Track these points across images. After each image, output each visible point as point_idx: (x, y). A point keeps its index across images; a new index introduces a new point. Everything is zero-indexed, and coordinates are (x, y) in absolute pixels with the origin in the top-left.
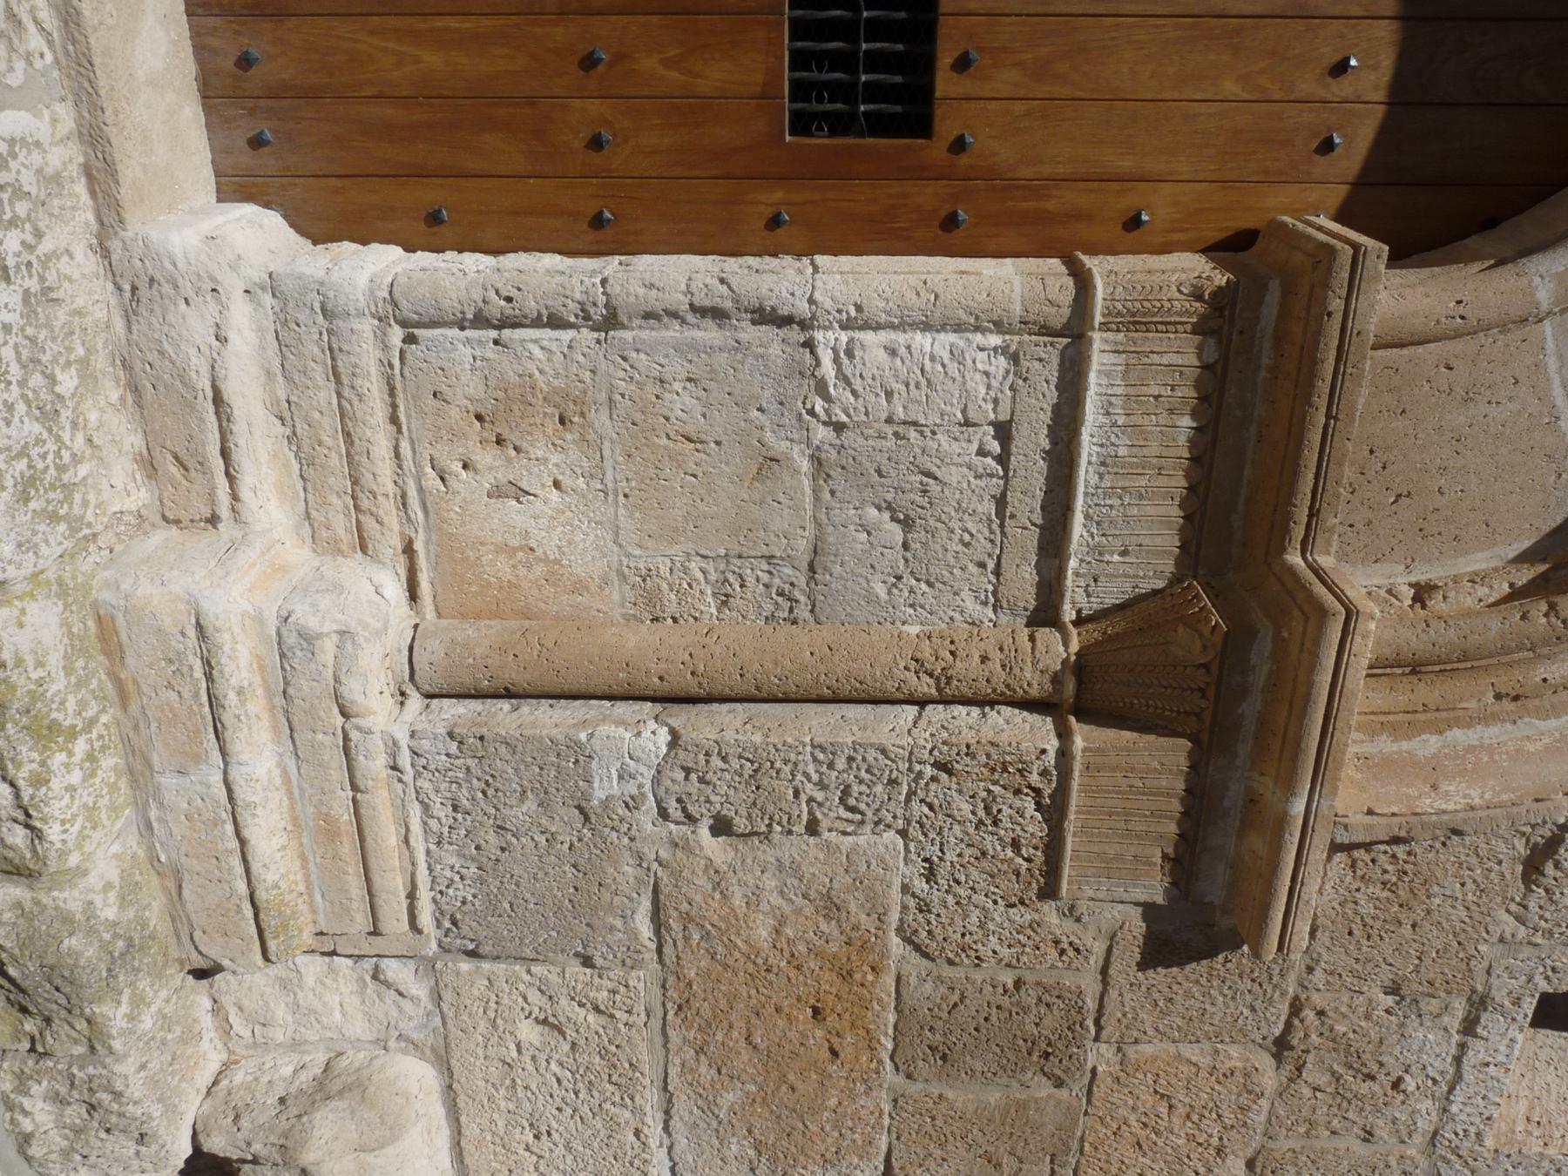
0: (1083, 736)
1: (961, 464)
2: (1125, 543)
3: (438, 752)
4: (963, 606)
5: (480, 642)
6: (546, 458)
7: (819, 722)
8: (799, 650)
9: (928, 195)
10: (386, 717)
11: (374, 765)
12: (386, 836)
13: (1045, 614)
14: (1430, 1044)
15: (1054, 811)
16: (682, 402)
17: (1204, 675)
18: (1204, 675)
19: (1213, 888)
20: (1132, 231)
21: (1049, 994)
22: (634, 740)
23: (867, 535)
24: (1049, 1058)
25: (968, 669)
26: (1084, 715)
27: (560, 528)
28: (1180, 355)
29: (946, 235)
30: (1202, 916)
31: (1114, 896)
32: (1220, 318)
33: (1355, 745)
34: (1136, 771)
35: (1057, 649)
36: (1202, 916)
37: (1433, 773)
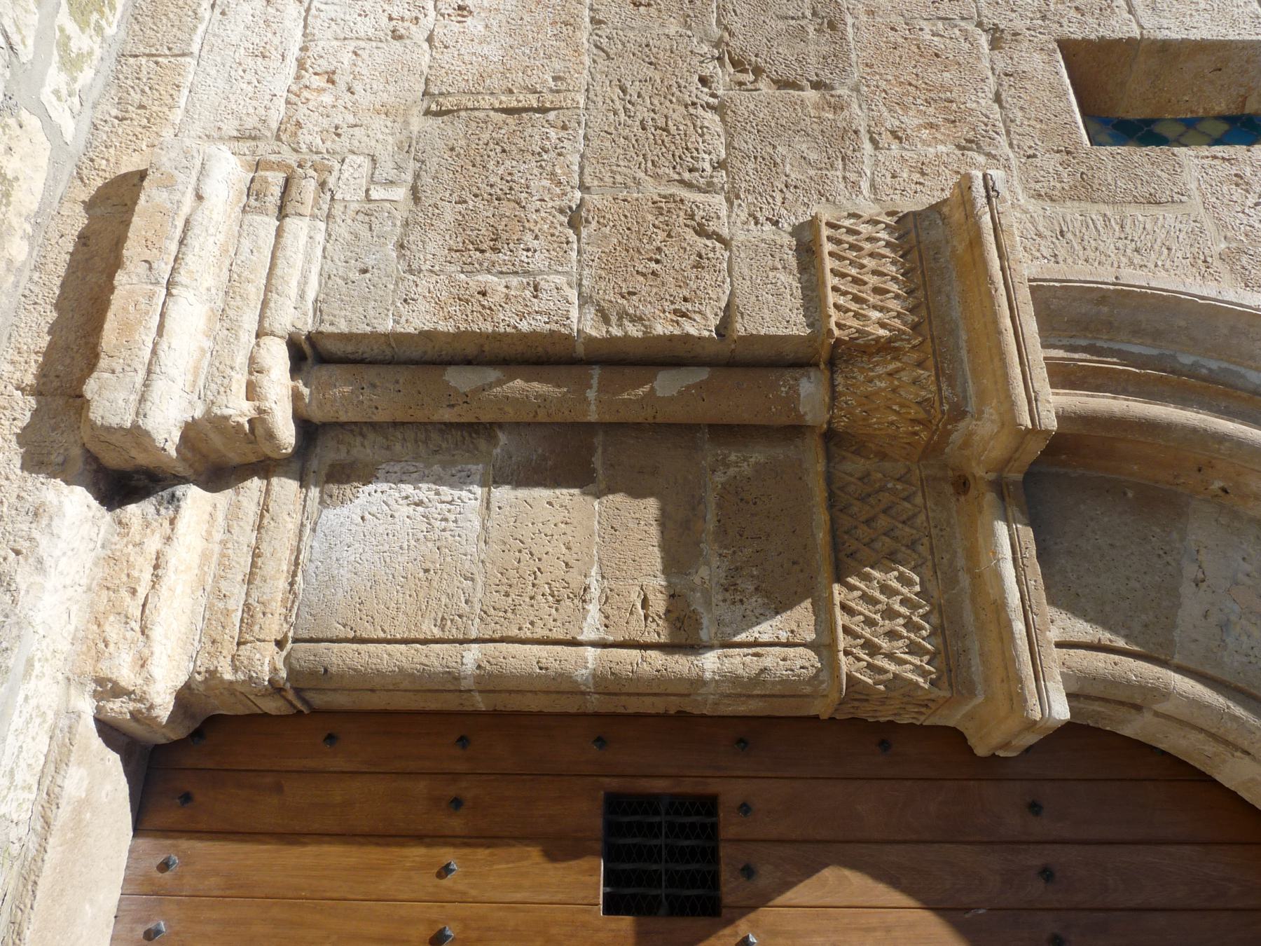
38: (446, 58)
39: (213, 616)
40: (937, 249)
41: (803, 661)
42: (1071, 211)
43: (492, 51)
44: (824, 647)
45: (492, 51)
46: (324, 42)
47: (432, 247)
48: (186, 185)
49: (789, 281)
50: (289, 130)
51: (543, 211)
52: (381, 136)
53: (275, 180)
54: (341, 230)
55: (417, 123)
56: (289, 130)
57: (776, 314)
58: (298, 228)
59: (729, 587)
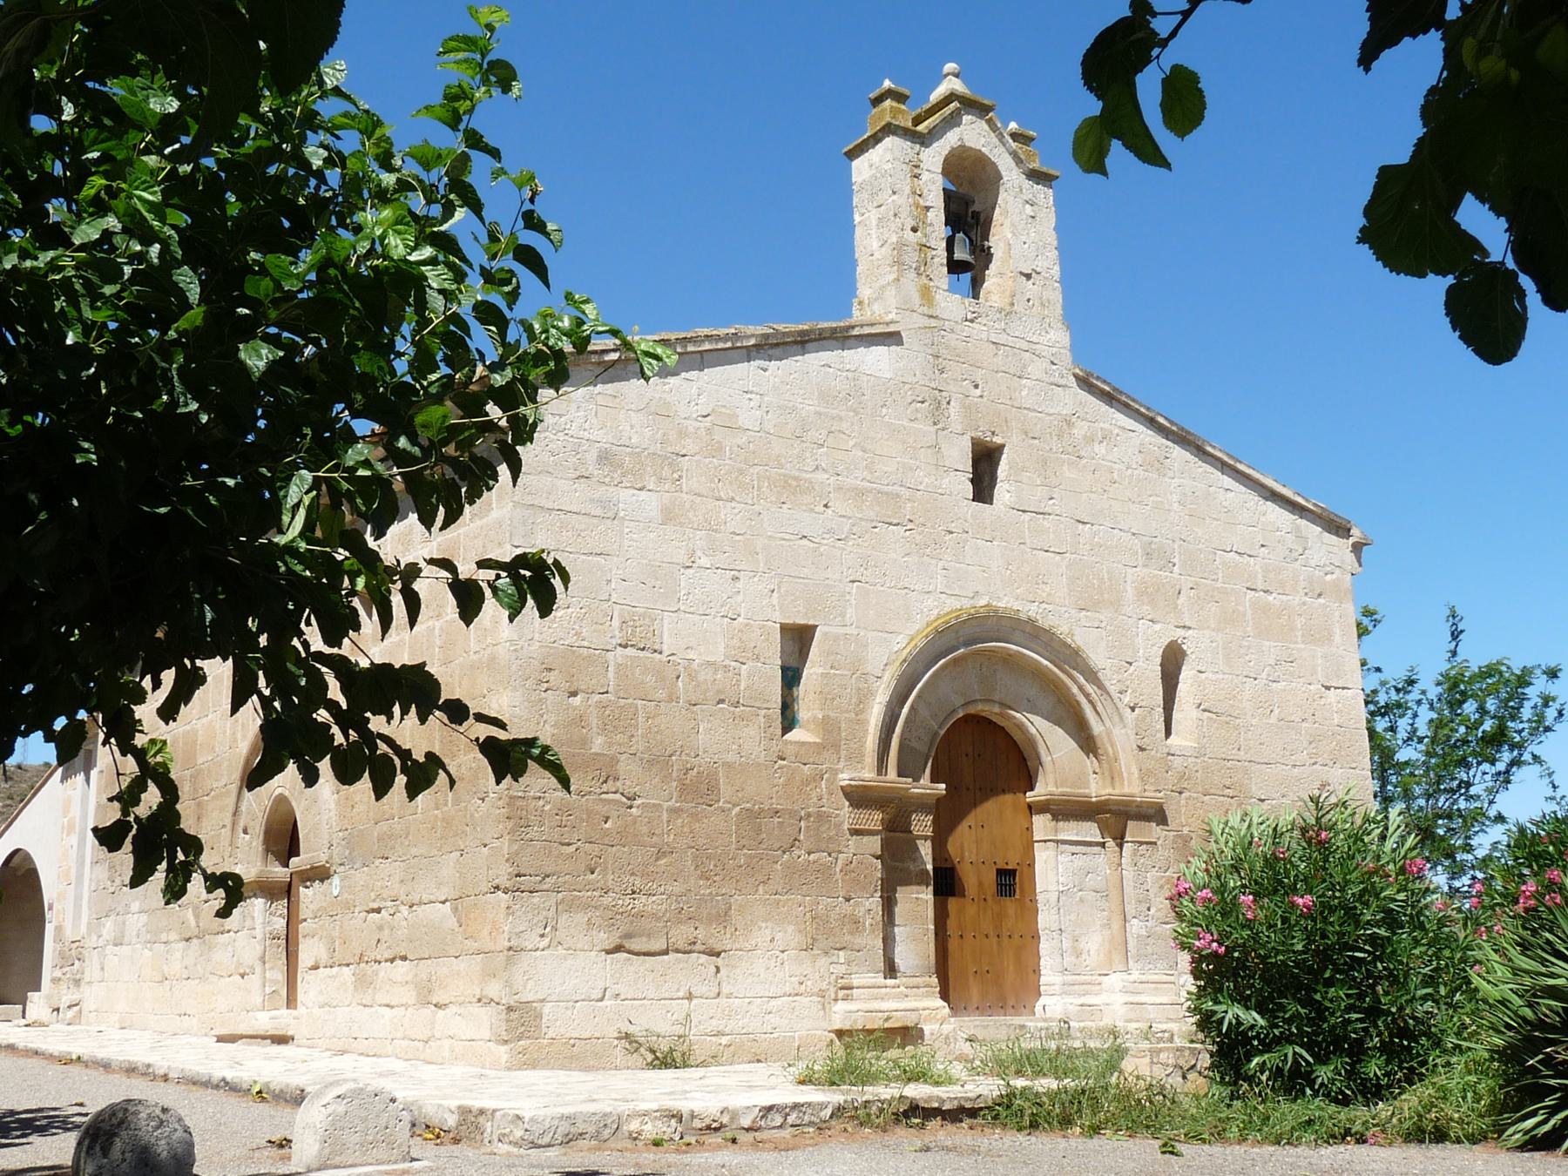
0: (1127, 838)
1: (1080, 861)
2: (1090, 831)
3: (1139, 965)
4: (1102, 861)
5: (1117, 957)
6: (1082, 945)
7: (1128, 889)
8: (1114, 894)
9: (1025, 868)
10: (1135, 976)
11: (1144, 978)
12: (1156, 978)
13: (1103, 845)
14: (1177, 762)
15: (1141, 843)
16: (1073, 917)
17: (1116, 819)
18: (1116, 819)
19: (1152, 811)
20: (1029, 829)
21: (1174, 842)
22: (1135, 926)
23: (1090, 881)
24: (1186, 840)
25: (1116, 860)
26: (1122, 837)
27: (1094, 943)
28: (1061, 824)
29: (1031, 865)
30: (1157, 815)
31: (1154, 831)
32: (1056, 817)
33: (1126, 790)
34: (1133, 829)
35: (1111, 843)
36: (1157, 815)
37: (1130, 774)
38: (793, 944)
39: (928, 995)
40: (859, 797)
41: (929, 843)
42: (843, 753)
43: (791, 928)
44: (926, 838)
45: (791, 928)
46: (788, 989)
47: (859, 941)
48: (854, 1016)
49: (866, 839)
50: (822, 994)
51: (847, 908)
52: (823, 962)
53: (841, 993)
54: (855, 969)
55: (816, 952)
56: (822, 994)
57: (875, 843)
58: (855, 983)
59: (914, 860)
